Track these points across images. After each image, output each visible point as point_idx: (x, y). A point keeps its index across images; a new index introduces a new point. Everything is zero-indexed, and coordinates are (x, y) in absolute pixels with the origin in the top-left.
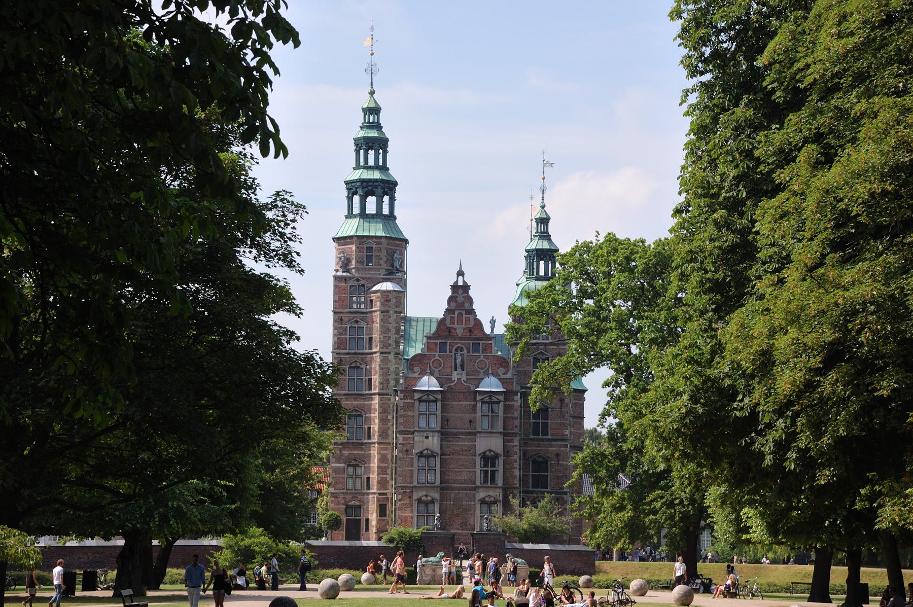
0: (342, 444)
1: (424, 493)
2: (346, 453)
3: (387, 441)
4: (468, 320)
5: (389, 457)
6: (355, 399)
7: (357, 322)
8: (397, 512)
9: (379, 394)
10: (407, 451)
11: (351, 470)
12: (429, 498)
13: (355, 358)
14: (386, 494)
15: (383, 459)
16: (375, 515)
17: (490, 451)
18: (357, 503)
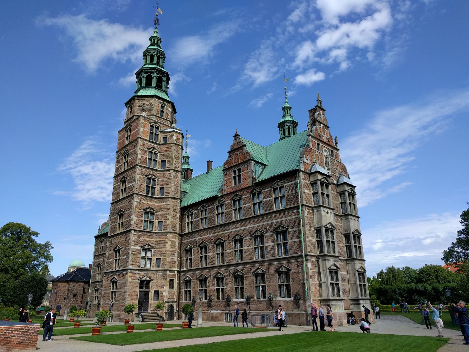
0: (140, 231)
1: (332, 263)
2: (142, 239)
3: (175, 232)
4: (327, 133)
5: (177, 244)
6: (150, 201)
7: (154, 148)
8: (310, 280)
9: (172, 198)
10: (310, 224)
11: (143, 254)
12: (335, 268)
13: (152, 172)
14: (174, 271)
15: (173, 245)
16: (166, 288)
17: (357, 231)
18: (148, 279)
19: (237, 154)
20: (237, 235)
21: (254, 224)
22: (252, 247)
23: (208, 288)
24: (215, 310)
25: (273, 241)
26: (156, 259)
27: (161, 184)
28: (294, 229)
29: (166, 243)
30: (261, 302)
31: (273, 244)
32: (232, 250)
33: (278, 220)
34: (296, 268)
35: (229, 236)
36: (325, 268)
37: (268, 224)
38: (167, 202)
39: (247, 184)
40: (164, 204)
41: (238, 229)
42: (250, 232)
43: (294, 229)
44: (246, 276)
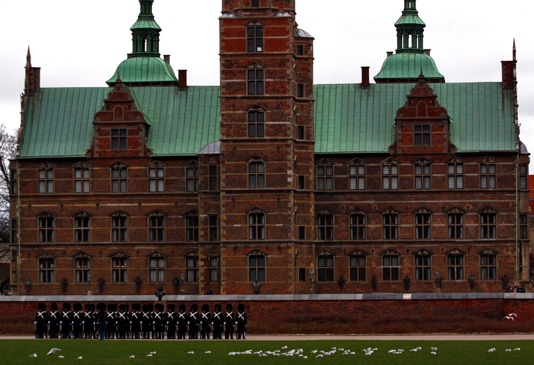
19: (423, 105)
20: (423, 208)
21: (450, 200)
22: (444, 225)
23: (367, 267)
24: (382, 292)
25: (476, 222)
26: (300, 227)
27: (299, 120)
28: (505, 214)
29: (310, 206)
30: (456, 284)
31: (477, 225)
32: (412, 225)
33: (486, 201)
34: (504, 251)
35: (406, 208)
36: (527, 253)
37: (471, 203)
38: (307, 148)
39: (442, 150)
40: (304, 151)
41: (422, 201)
42: (443, 208)
43: (505, 214)
44: (434, 255)
